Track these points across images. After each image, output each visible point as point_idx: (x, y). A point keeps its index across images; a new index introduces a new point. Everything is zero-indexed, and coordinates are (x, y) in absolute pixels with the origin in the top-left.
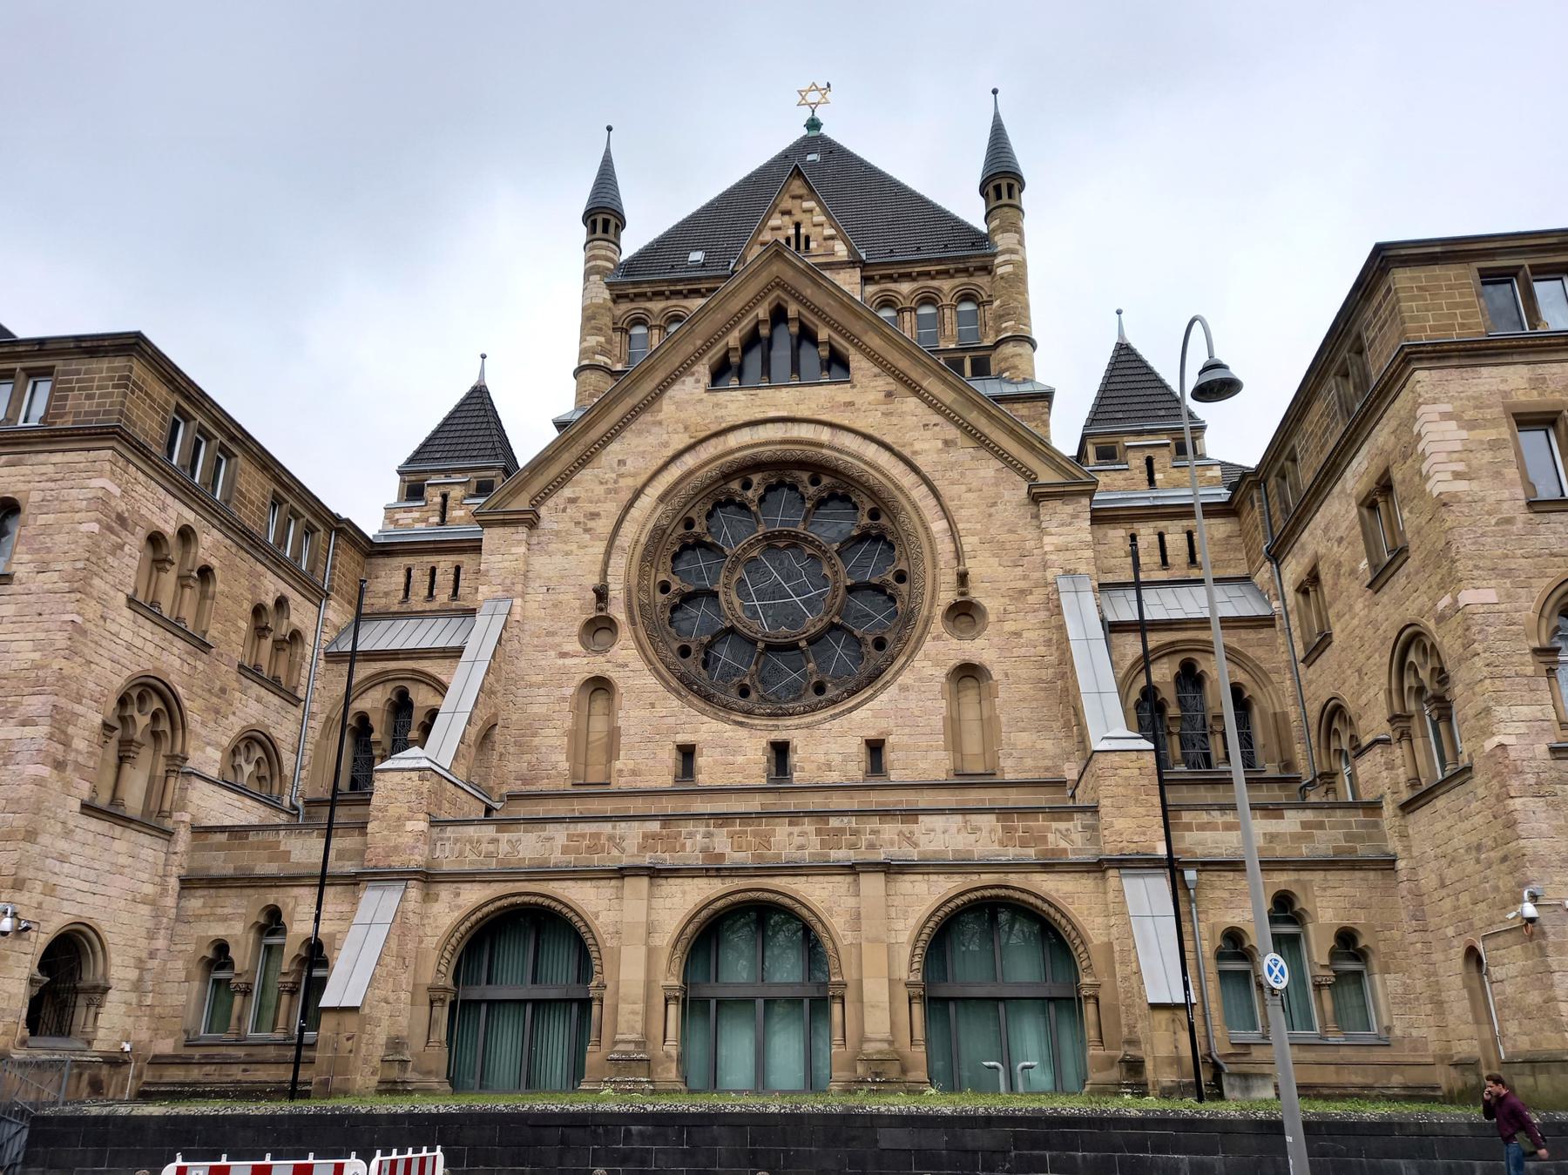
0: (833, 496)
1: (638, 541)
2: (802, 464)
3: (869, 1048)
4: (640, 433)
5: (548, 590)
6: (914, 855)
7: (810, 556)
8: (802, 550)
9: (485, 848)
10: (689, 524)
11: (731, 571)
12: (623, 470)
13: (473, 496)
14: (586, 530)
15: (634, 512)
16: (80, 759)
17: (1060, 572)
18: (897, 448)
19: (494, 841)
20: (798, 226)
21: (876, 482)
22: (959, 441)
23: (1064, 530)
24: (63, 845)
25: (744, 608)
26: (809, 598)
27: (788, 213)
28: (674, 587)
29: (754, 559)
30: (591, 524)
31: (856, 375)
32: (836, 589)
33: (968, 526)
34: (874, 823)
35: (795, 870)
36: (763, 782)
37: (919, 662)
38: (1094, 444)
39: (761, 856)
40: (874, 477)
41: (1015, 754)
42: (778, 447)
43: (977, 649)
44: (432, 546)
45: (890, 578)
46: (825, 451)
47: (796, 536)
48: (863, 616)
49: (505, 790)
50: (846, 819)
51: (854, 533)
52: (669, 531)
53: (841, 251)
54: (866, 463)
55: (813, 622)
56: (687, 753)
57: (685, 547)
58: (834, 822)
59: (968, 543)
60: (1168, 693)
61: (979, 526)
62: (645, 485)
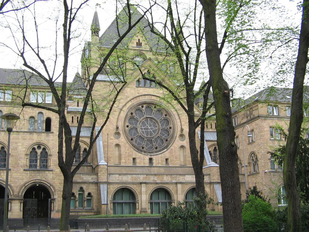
2: (153, 104)
9: (117, 178)
10: (132, 114)
11: (140, 124)
19: (119, 177)
25: (142, 131)
28: (130, 127)
29: (143, 121)
32: (159, 129)
35: (167, 183)
36: (148, 165)
37: (174, 145)
56: (134, 159)
60: (212, 152)
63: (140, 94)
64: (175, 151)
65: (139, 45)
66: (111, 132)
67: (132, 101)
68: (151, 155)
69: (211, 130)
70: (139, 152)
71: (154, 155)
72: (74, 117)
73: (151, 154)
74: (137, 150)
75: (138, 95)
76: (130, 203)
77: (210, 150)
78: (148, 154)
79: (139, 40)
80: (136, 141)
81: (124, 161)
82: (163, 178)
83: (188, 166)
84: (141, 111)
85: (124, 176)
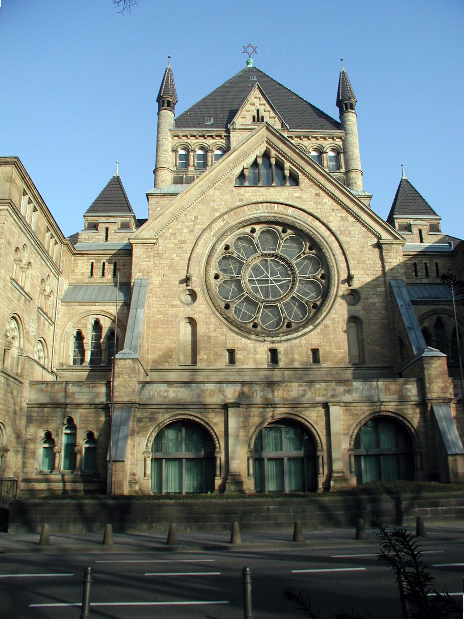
5: (163, 276)
13: (119, 229)
18: (322, 219)
27: (254, 104)
28: (221, 277)
31: (302, 185)
36: (266, 366)
44: (103, 252)
49: (150, 368)
56: (232, 352)
57: (224, 258)
63: (246, 203)
64: (334, 330)
65: (258, 121)
66: (174, 289)
67: (225, 217)
68: (273, 342)
69: (425, 281)
70: (244, 334)
71: (280, 342)
72: (94, 264)
73: (274, 339)
74: (237, 330)
75: (240, 204)
76: (180, 460)
77: (426, 324)
78: (266, 339)
79: (258, 111)
80: (237, 311)
81: (206, 357)
83: (370, 365)
85: (181, 387)
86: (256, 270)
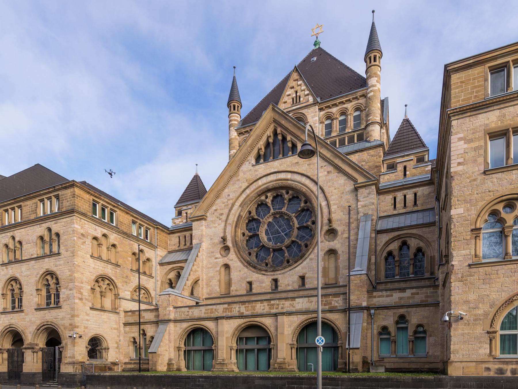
0: (294, 197)
1: (233, 221)
3: (278, 361)
4: (233, 184)
6: (294, 310)
7: (287, 219)
8: (284, 218)
12: (229, 198)
14: (220, 219)
15: (233, 211)
16: (86, 297)
17: (362, 215)
18: (311, 177)
20: (296, 92)
21: (305, 190)
22: (332, 171)
23: (365, 199)
24: (87, 317)
26: (286, 233)
28: (246, 234)
30: (221, 217)
33: (334, 202)
34: (283, 302)
38: (386, 163)
39: (253, 313)
40: (304, 189)
41: (343, 277)
42: (275, 182)
43: (336, 244)
45: (309, 223)
46: (289, 182)
47: (282, 212)
48: (302, 237)
50: (275, 301)
51: (299, 209)
52: (243, 216)
53: (311, 99)
54: (302, 184)
55: (287, 242)
58: (272, 302)
59: (333, 208)
61: (337, 202)
62: (235, 202)
82: (254, 308)
84: (266, 205)
86: (269, 224)
